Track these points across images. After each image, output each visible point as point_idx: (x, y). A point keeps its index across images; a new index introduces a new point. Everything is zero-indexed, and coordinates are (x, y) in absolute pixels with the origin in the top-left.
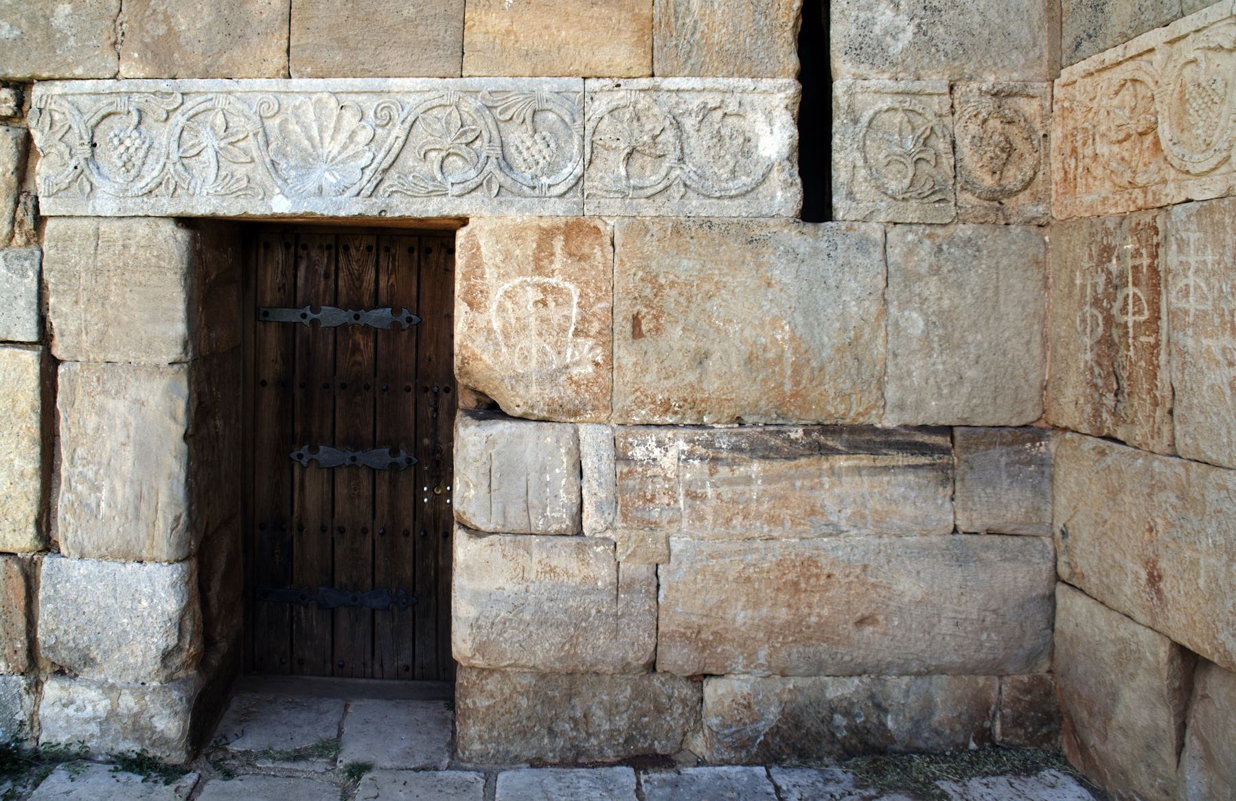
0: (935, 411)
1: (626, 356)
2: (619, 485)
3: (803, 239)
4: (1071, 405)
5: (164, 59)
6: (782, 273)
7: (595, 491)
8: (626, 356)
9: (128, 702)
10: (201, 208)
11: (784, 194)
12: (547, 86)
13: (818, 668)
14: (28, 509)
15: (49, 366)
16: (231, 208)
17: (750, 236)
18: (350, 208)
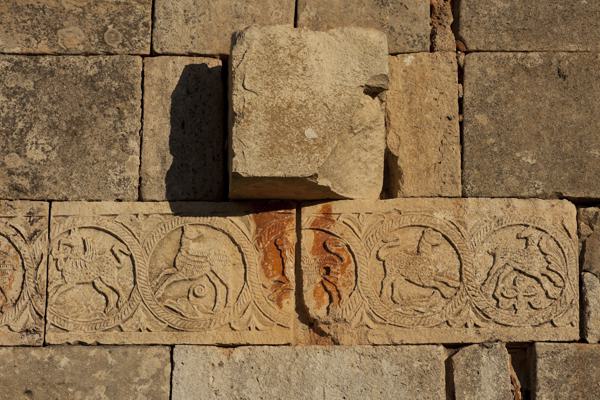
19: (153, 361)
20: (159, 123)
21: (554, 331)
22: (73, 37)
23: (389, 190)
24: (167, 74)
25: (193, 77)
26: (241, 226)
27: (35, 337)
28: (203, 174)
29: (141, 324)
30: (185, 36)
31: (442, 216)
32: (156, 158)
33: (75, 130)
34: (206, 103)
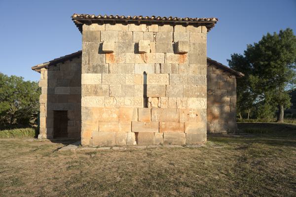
19: (133, 65)
20: (133, 47)
21: (162, 63)
22: (127, 41)
23: (150, 52)
24: (134, 43)
25: (136, 43)
26: (140, 55)
27: (125, 63)
28: (137, 51)
29: (133, 62)
30: (135, 41)
31: (154, 54)
32: (133, 49)
33: (128, 47)
34: (137, 46)
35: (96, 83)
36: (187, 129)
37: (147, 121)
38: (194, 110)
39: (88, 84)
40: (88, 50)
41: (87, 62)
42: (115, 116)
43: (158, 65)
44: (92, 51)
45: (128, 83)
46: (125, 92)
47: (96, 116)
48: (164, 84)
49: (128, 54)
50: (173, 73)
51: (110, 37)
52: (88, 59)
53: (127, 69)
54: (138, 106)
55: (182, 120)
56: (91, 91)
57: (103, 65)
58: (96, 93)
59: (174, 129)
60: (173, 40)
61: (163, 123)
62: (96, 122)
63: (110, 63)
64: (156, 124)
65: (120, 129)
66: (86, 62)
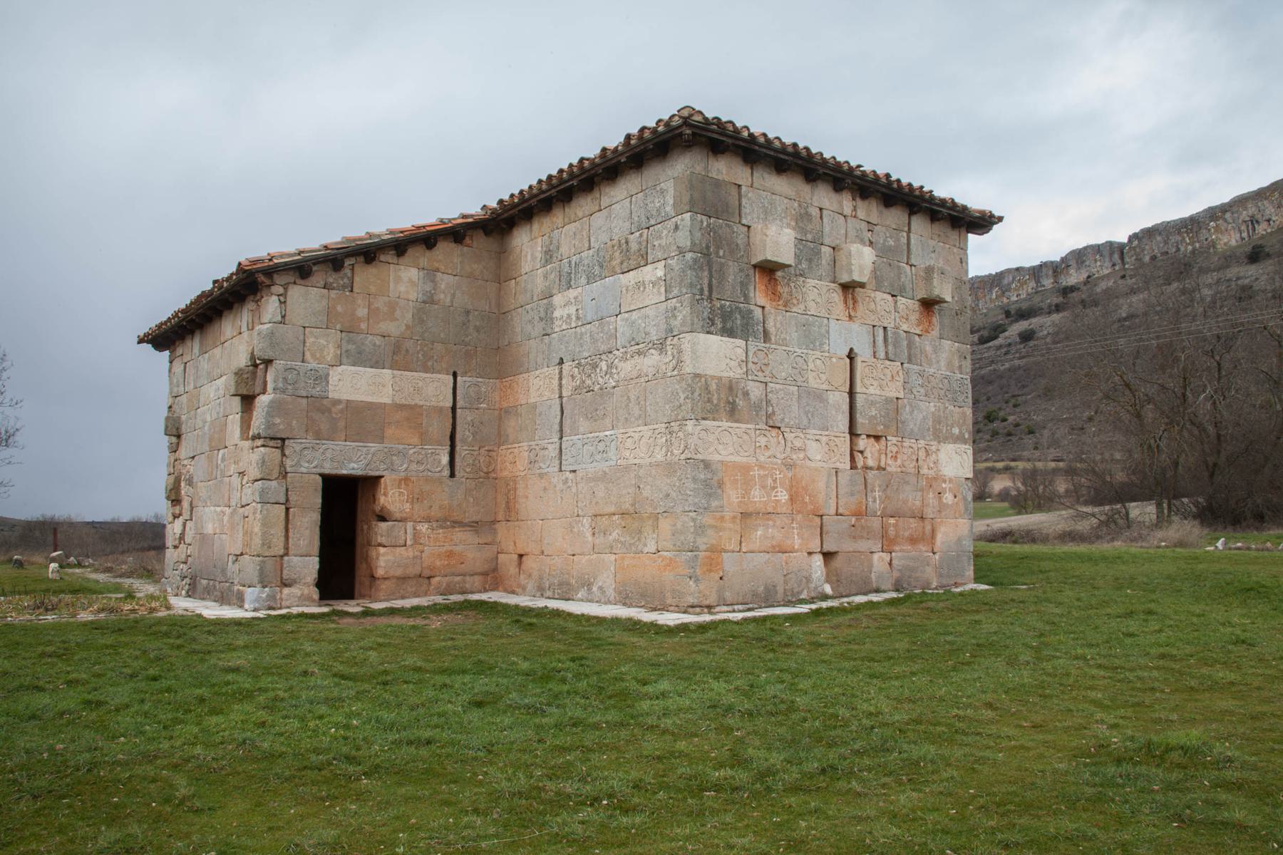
0: (474, 519)
1: (416, 506)
2: (414, 535)
3: (449, 482)
4: (500, 517)
5: (318, 436)
6: (446, 489)
7: (409, 537)
8: (416, 506)
9: (306, 592)
10: (327, 471)
11: (447, 472)
12: (401, 447)
13: (453, 574)
14: (282, 545)
15: (287, 509)
16: (334, 472)
17: (440, 481)
18: (359, 473)
35: (732, 374)
36: (939, 538)
37: (858, 514)
38: (951, 481)
39: (710, 372)
40: (708, 247)
41: (706, 293)
42: (783, 496)
43: (881, 331)
44: (717, 253)
45: (813, 383)
46: (806, 413)
47: (732, 496)
48: (894, 395)
49: (811, 282)
50: (910, 362)
51: (766, 213)
52: (706, 281)
53: (813, 338)
54: (838, 465)
55: (929, 513)
56: (719, 399)
57: (751, 312)
58: (733, 412)
59: (913, 541)
60: (908, 258)
61: (892, 521)
62: (734, 517)
63: (768, 308)
64: (876, 523)
65: (797, 543)
66: (702, 289)
